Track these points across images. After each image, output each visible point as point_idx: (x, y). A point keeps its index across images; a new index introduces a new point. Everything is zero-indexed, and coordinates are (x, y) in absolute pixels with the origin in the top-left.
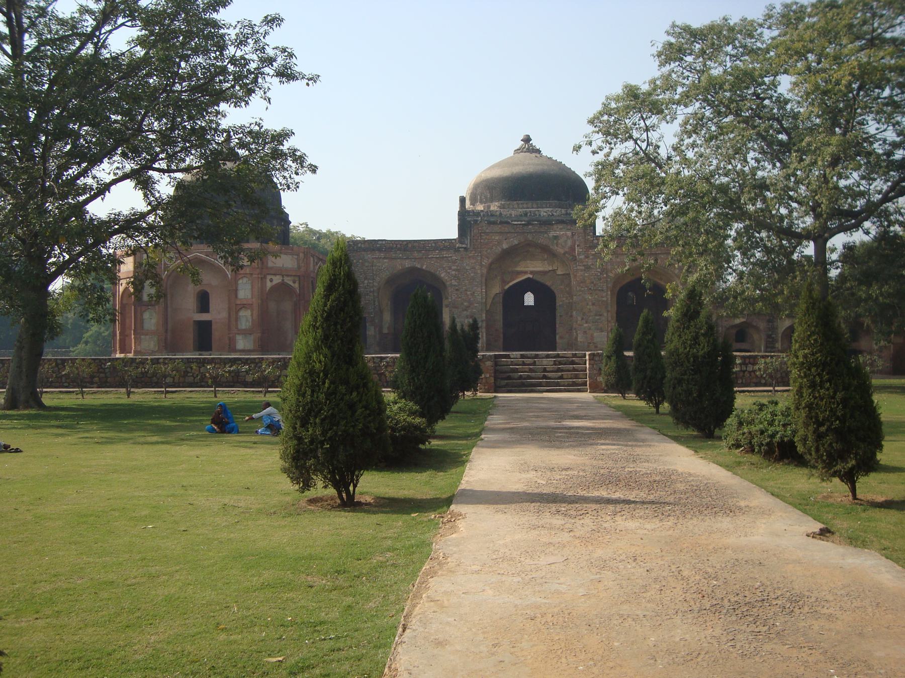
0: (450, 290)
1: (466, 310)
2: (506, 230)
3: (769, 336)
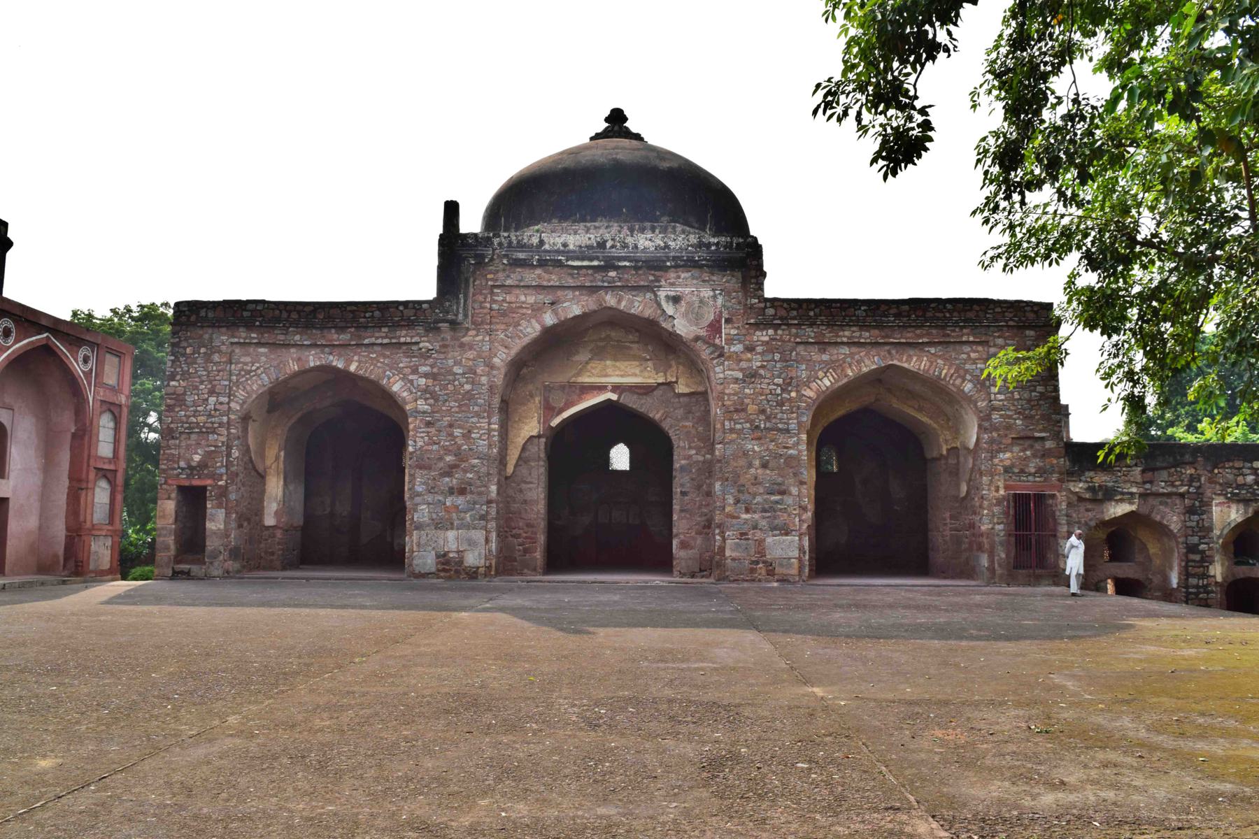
0: (413, 423)
2: (554, 279)
3: (1192, 549)
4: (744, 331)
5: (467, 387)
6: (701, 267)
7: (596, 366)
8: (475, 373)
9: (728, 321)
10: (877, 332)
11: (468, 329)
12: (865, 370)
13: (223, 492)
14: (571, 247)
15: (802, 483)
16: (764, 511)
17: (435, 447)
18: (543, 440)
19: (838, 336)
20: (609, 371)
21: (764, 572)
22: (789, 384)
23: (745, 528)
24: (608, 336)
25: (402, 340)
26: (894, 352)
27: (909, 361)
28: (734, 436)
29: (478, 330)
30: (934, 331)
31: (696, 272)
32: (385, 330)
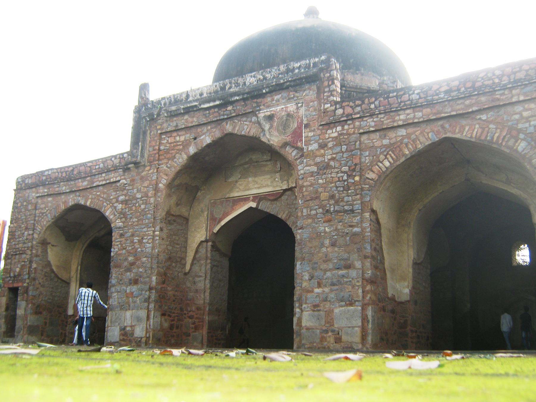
1: (129, 270)
4: (319, 132)
5: (143, 207)
6: (287, 88)
7: (242, 184)
8: (147, 196)
9: (307, 126)
10: (428, 110)
11: (144, 166)
12: (420, 147)
13: (26, 291)
14: (205, 95)
15: (366, 257)
16: (333, 284)
17: (124, 251)
18: (210, 244)
19: (394, 122)
20: (251, 185)
21: (332, 340)
22: (354, 170)
23: (317, 301)
24: (251, 159)
25: (112, 180)
26: (447, 126)
27: (461, 132)
28: (310, 221)
29: (150, 166)
30: (483, 99)
31: (285, 94)
32: (104, 175)
